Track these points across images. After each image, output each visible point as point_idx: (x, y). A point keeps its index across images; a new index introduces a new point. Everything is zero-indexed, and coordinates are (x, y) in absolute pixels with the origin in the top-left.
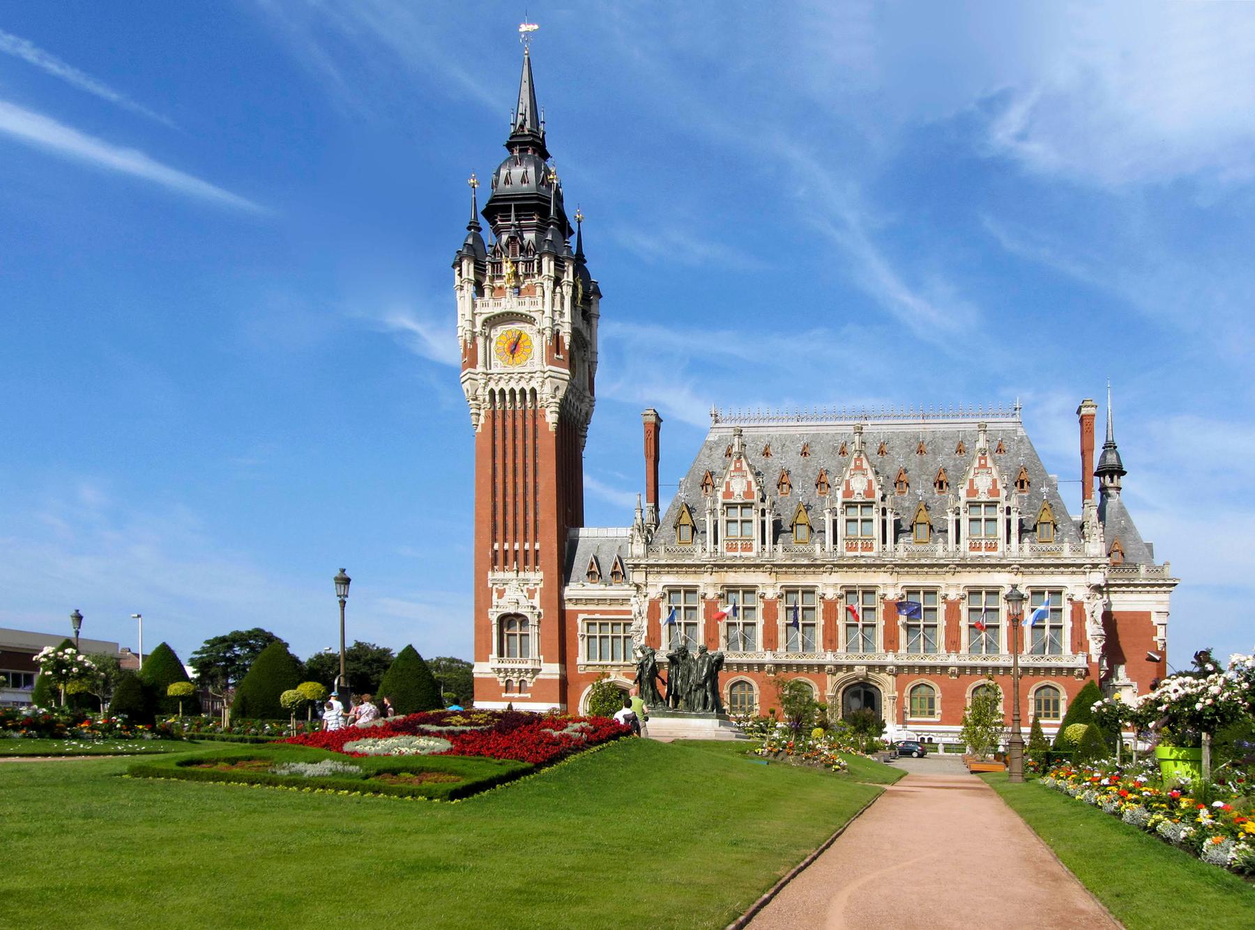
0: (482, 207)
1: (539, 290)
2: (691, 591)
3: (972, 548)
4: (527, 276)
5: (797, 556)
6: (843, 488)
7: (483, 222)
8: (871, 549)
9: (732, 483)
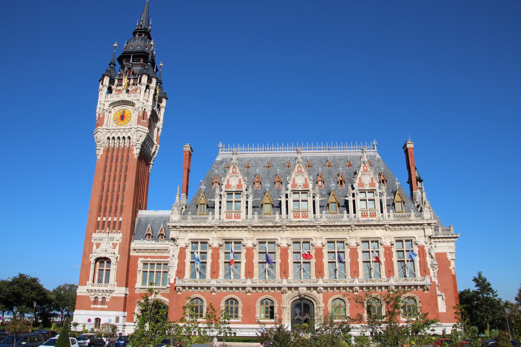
0: (118, 56)
1: (138, 91)
2: (204, 242)
3: (362, 216)
4: (134, 84)
5: (265, 221)
6: (291, 182)
7: (117, 63)
8: (307, 217)
9: (231, 179)
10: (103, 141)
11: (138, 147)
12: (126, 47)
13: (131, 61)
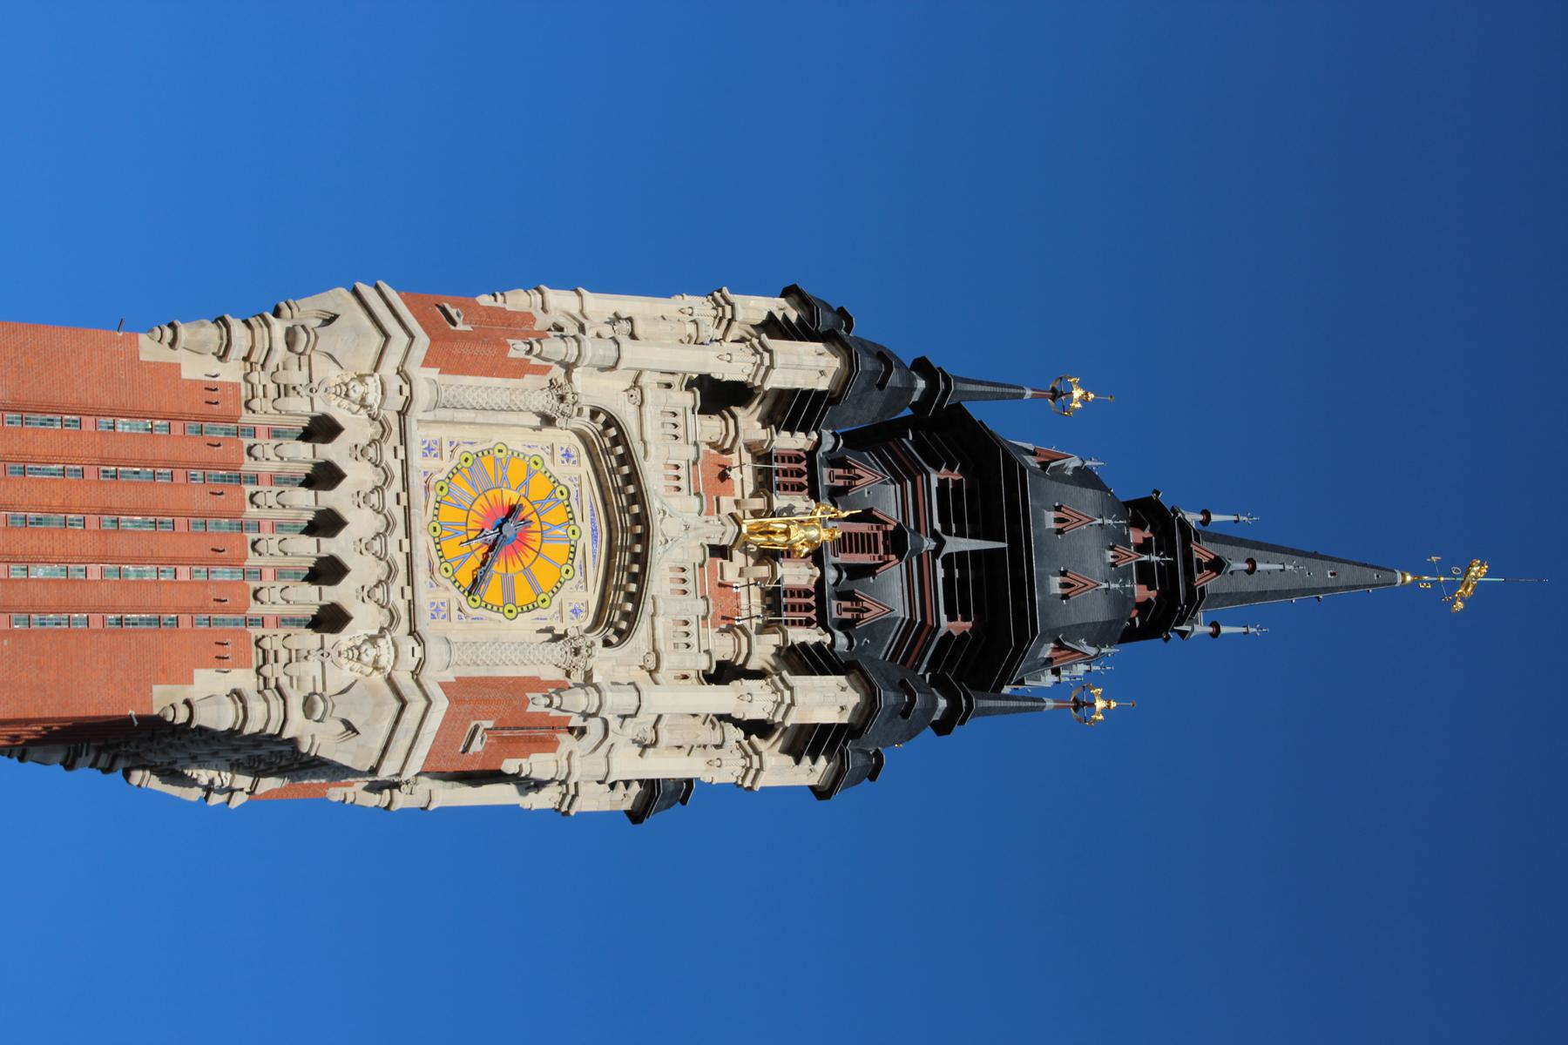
4: (774, 598)
10: (296, 377)
11: (257, 709)
12: (1058, 475)
13: (955, 545)
